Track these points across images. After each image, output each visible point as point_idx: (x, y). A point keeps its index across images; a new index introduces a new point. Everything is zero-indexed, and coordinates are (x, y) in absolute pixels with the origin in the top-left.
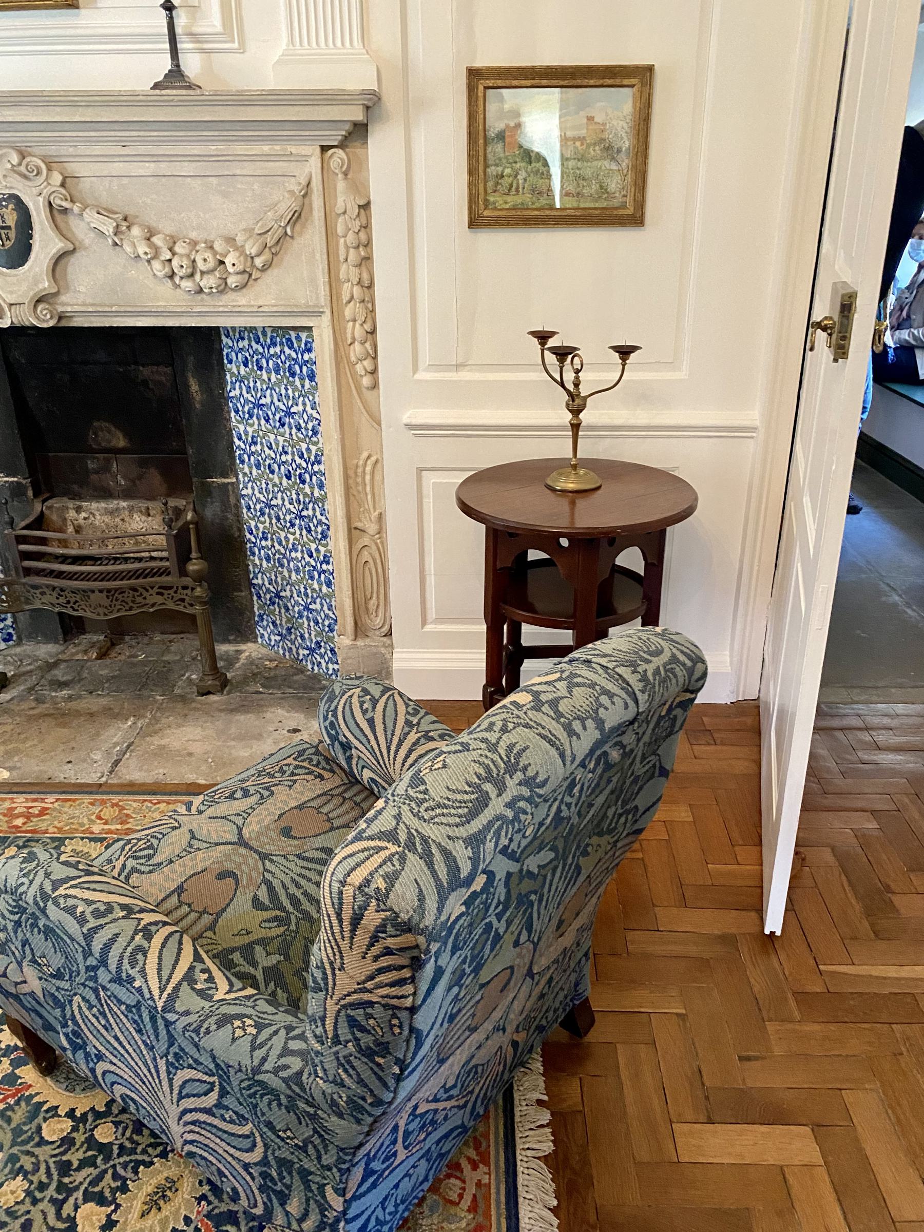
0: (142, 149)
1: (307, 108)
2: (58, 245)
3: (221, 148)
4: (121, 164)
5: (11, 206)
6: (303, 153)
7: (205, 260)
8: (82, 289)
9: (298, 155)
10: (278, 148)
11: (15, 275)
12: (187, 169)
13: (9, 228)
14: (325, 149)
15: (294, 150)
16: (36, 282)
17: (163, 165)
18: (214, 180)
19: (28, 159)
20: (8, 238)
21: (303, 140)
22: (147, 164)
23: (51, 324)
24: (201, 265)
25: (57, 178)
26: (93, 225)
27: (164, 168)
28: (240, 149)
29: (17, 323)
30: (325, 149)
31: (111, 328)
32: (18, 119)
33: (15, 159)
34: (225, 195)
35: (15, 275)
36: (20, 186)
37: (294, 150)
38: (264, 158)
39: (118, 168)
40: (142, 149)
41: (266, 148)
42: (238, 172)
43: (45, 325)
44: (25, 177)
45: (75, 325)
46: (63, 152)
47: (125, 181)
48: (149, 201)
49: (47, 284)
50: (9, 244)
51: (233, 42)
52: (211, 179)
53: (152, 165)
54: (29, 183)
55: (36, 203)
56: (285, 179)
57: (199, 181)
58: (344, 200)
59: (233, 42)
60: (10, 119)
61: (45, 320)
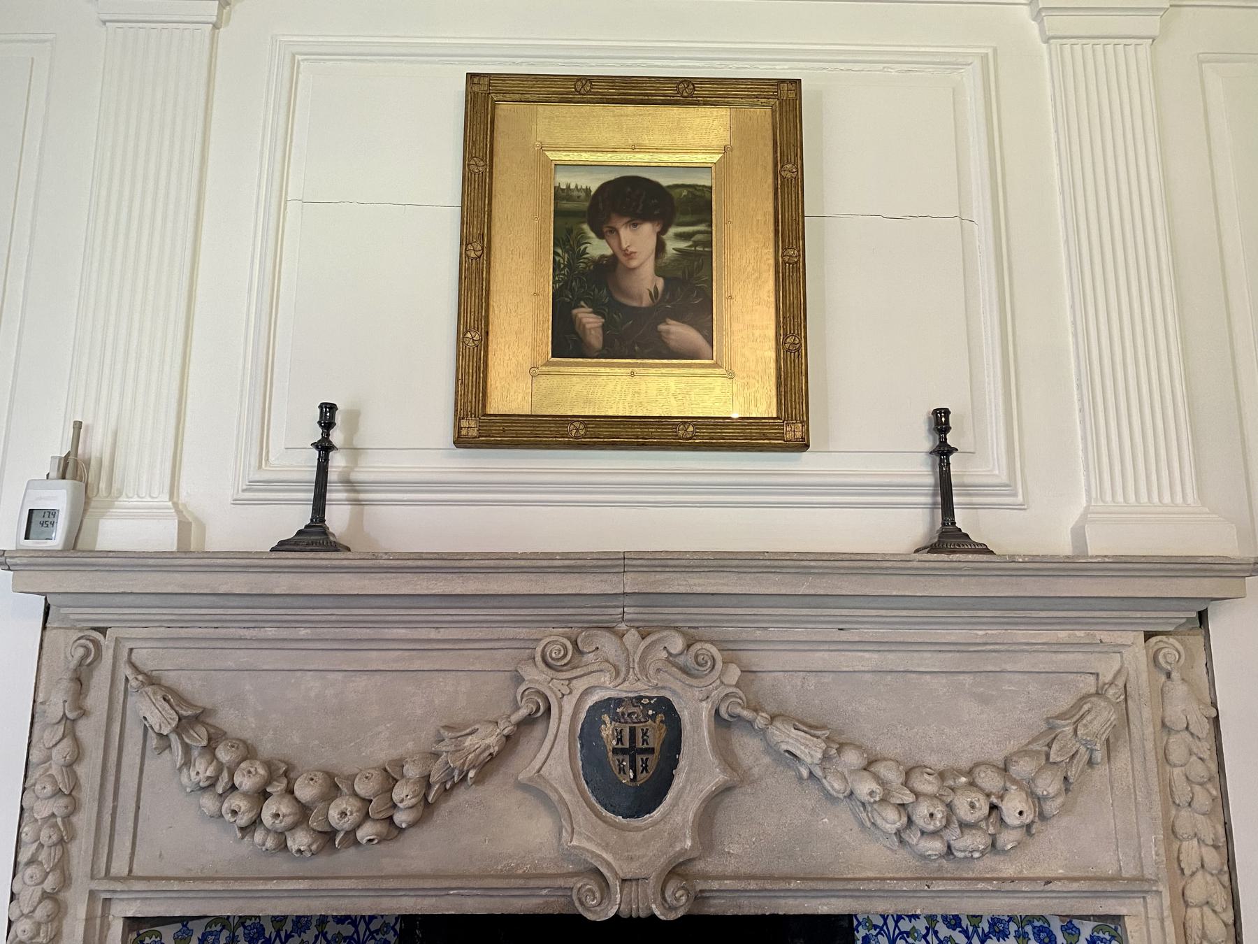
0: (870, 633)
1: (1160, 582)
2: (716, 777)
3: (994, 632)
4: (826, 655)
5: (660, 717)
6: (1120, 641)
7: (972, 806)
8: (734, 849)
9: (1110, 645)
10: (1081, 634)
11: (638, 829)
12: (929, 661)
13: (651, 751)
14: (1148, 636)
15: (1105, 636)
16: (674, 838)
17: (891, 656)
18: (968, 680)
19: (698, 646)
20: (645, 769)
21: (1120, 624)
22: (867, 655)
23: (680, 913)
24: (963, 811)
25: (734, 674)
26: (784, 747)
27: (893, 660)
28: (1022, 635)
29: (625, 914)
30: (1148, 636)
31: (774, 917)
32: (725, 590)
33: (677, 644)
34: (984, 700)
35: (638, 829)
36: (677, 686)
37: (1105, 636)
38: (1055, 648)
39: (819, 659)
40: (870, 633)
41: (1063, 635)
42: (1009, 667)
43: (672, 916)
44: (685, 670)
45: (712, 911)
46: (744, 636)
47: (828, 678)
48: (862, 709)
49: (689, 843)
50: (643, 777)
51: (1015, 495)
52: (961, 677)
53: (875, 656)
54: (694, 682)
55: (696, 714)
56: (1078, 677)
57: (943, 680)
58: (1182, 706)
59: (1015, 495)
60: (699, 590)
61: (669, 906)
